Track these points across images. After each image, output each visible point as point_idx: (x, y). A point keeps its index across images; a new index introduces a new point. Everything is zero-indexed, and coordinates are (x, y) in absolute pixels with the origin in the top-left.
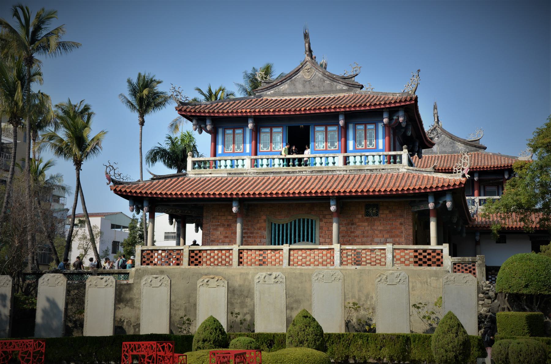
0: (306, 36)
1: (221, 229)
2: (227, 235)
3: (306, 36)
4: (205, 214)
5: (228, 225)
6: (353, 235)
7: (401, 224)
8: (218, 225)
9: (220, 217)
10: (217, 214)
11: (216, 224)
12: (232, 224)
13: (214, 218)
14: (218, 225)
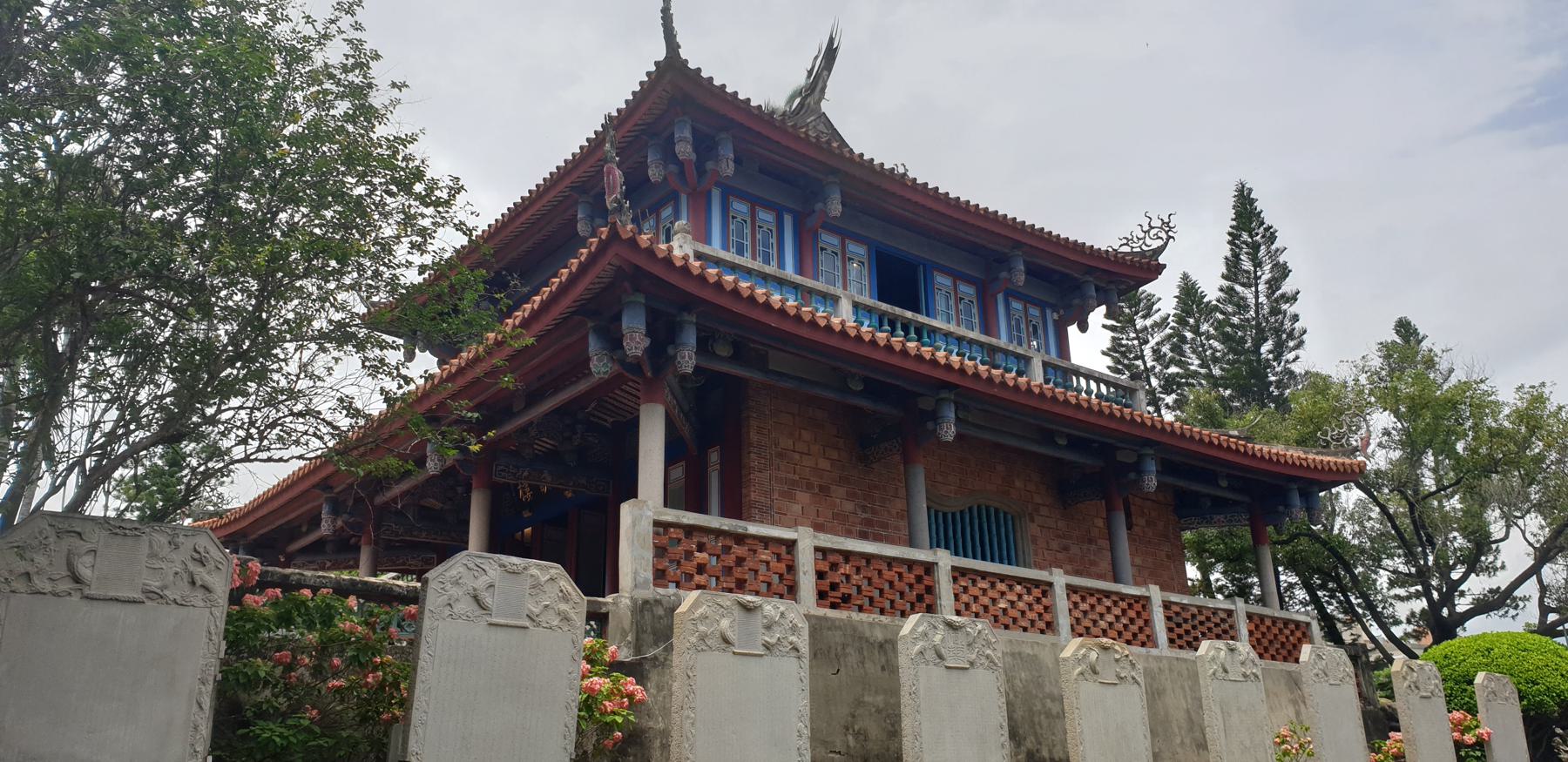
0: (830, 54)
1: (803, 497)
2: (821, 520)
3: (830, 54)
4: (754, 437)
5: (821, 488)
6: (1093, 569)
7: (1168, 556)
8: (794, 483)
9: (797, 456)
10: (790, 442)
11: (791, 476)
12: (833, 488)
13: (781, 455)
14: (794, 483)
